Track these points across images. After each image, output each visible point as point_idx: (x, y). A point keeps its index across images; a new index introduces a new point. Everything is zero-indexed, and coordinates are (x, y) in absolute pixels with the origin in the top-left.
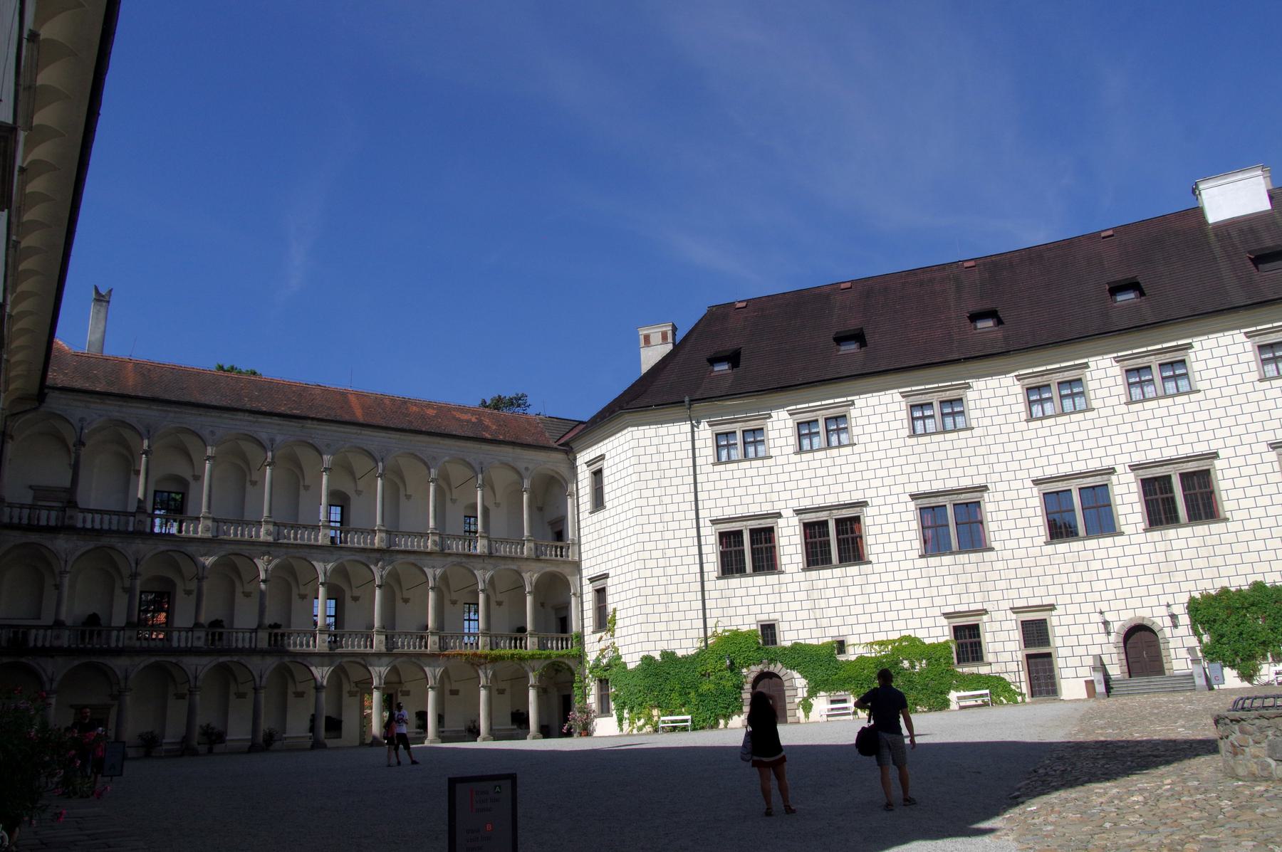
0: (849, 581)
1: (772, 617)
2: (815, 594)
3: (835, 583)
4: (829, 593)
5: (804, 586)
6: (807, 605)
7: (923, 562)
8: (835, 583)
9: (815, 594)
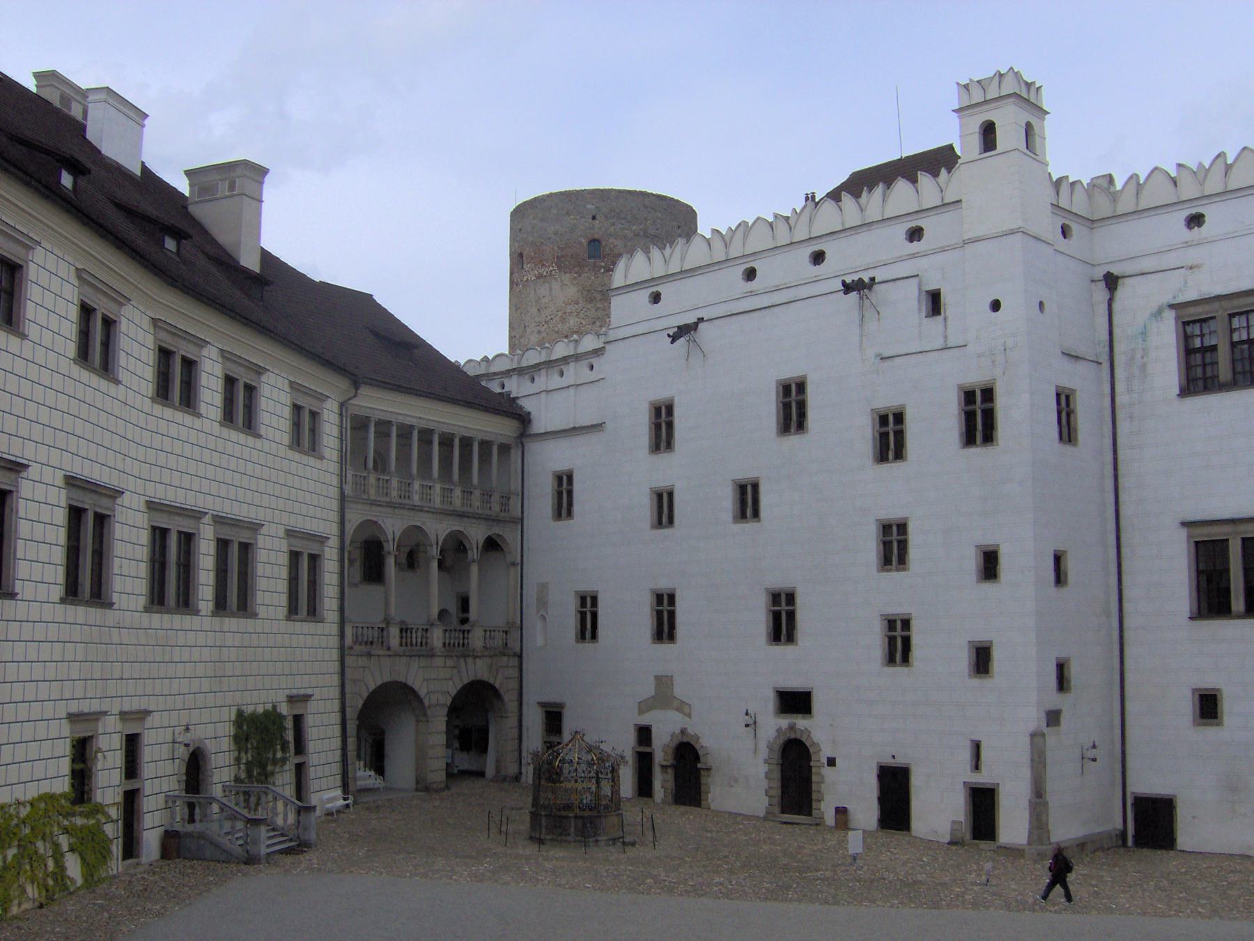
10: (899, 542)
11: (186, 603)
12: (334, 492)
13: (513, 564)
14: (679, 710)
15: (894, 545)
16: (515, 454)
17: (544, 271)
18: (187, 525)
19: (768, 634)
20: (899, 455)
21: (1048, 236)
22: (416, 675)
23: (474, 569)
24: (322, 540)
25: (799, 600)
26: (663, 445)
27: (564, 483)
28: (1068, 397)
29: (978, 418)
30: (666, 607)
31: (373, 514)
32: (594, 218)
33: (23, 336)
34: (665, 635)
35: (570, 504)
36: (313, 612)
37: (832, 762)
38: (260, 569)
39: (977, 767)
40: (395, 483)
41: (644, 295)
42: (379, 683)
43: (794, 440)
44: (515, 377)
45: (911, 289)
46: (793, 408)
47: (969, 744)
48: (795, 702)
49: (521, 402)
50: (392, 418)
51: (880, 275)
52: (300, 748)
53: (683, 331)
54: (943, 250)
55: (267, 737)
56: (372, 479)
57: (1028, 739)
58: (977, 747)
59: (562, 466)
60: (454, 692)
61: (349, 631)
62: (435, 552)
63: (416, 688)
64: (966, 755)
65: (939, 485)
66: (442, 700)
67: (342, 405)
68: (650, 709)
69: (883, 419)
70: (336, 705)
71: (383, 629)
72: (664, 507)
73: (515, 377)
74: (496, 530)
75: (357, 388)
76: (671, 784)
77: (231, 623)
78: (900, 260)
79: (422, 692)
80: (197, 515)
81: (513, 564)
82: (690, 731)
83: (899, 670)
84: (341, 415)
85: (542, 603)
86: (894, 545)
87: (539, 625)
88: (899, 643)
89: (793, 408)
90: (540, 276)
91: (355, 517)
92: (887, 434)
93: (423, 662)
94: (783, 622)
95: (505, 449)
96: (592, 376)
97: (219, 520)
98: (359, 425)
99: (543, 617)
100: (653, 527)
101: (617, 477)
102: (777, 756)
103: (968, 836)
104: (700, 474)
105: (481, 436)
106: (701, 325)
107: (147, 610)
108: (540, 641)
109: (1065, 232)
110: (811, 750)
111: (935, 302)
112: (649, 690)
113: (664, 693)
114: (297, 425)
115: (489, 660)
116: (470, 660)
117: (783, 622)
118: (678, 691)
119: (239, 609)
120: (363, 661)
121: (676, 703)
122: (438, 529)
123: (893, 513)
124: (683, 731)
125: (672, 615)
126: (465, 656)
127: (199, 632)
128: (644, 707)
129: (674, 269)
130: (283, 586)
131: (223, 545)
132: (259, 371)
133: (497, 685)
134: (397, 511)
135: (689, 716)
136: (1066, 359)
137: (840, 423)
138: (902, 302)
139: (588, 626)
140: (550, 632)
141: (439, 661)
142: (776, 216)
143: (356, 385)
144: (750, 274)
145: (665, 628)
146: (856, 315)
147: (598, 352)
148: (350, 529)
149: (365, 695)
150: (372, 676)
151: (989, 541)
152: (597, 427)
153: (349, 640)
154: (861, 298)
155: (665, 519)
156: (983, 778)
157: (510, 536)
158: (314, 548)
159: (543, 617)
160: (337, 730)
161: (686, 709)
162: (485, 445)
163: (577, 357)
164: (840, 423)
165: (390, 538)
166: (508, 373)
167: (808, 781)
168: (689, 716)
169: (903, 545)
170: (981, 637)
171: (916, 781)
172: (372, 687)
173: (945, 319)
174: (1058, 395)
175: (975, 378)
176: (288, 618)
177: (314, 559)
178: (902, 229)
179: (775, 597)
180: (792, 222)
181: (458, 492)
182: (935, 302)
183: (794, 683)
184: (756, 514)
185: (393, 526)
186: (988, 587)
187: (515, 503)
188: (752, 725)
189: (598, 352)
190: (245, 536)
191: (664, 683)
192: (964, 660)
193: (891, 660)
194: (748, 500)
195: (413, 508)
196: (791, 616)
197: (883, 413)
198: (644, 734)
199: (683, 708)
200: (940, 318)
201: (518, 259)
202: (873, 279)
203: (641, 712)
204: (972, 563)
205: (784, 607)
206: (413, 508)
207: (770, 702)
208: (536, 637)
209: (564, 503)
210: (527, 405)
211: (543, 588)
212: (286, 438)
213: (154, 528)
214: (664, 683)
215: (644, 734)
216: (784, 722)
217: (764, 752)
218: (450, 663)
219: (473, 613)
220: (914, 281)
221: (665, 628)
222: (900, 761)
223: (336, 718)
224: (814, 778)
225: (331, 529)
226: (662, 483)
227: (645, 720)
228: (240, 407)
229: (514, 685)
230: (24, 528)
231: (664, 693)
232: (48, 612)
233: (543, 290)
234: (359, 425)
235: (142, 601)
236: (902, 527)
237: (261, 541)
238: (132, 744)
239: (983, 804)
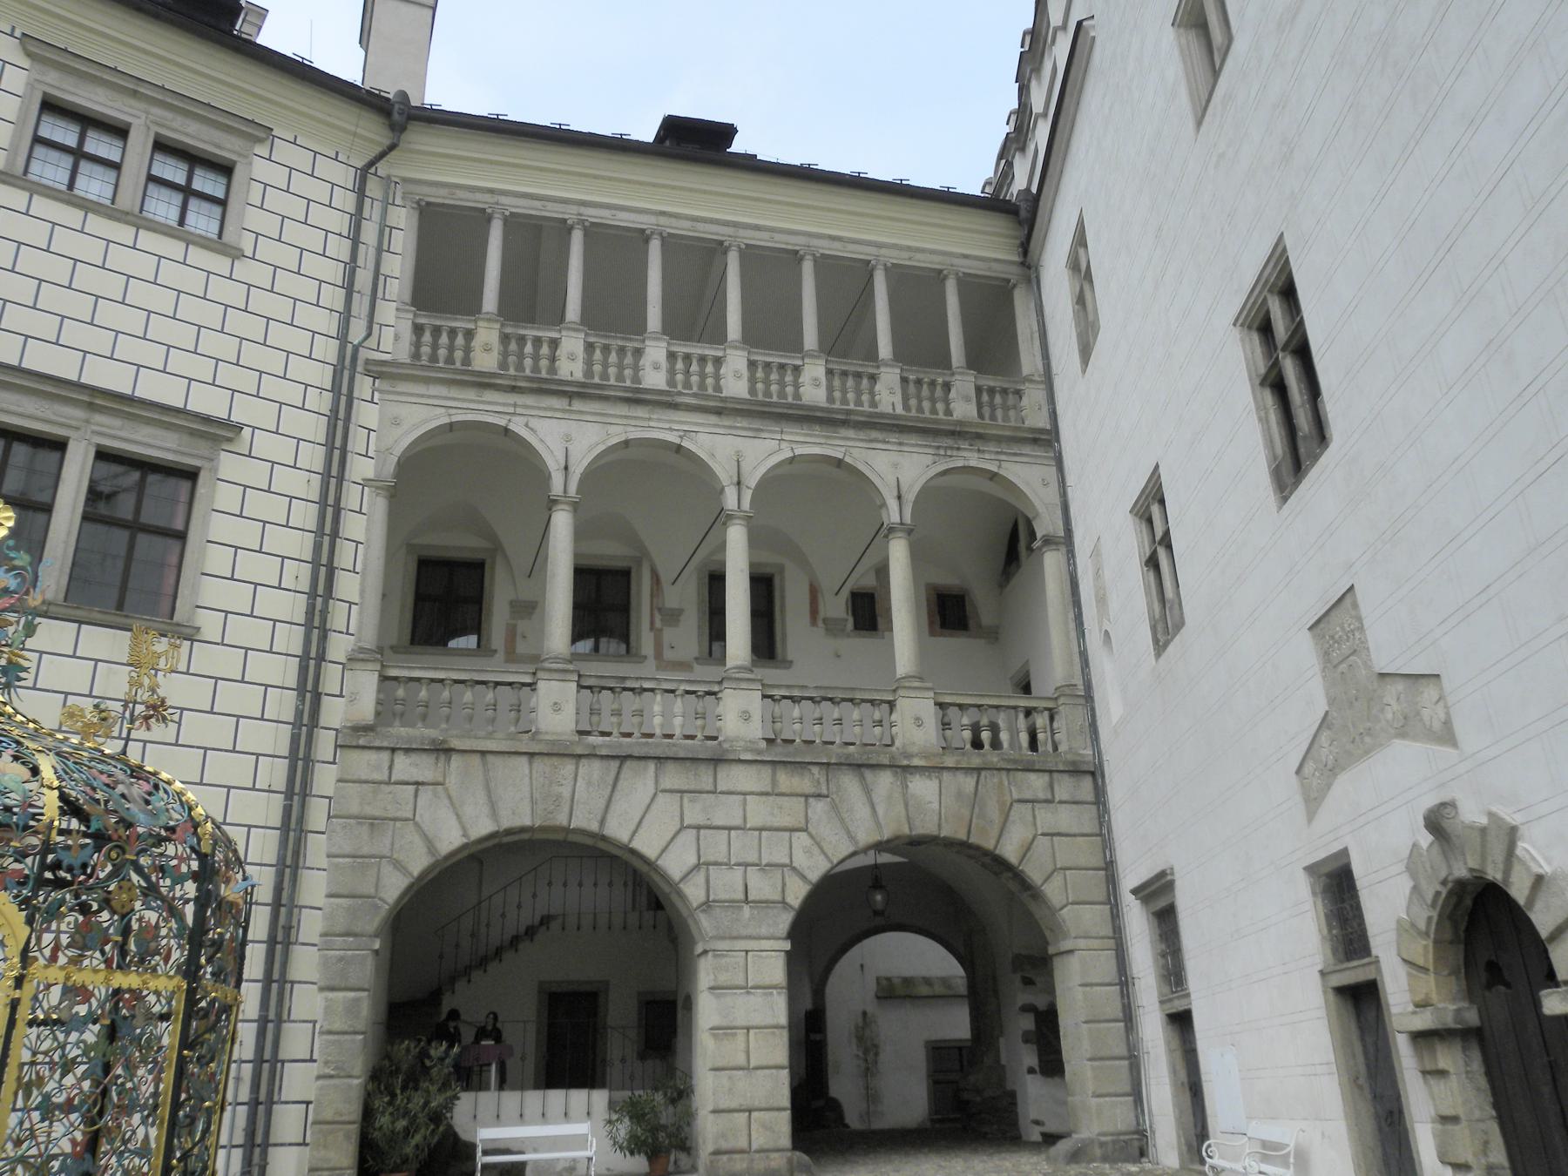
31: (489, 409)
50: (570, 213)
66: (763, 888)
81: (1049, 541)
84: (361, 193)
93: (674, 777)
115: (968, 783)
116: (884, 782)
122: (741, 457)
133: (1010, 851)
134: (578, 405)
135: (1446, 735)
157: (1026, 475)
165: (553, 464)
168: (1446, 735)
172: (450, 839)
206: (637, 398)
218: (786, 780)
229: (1084, 852)
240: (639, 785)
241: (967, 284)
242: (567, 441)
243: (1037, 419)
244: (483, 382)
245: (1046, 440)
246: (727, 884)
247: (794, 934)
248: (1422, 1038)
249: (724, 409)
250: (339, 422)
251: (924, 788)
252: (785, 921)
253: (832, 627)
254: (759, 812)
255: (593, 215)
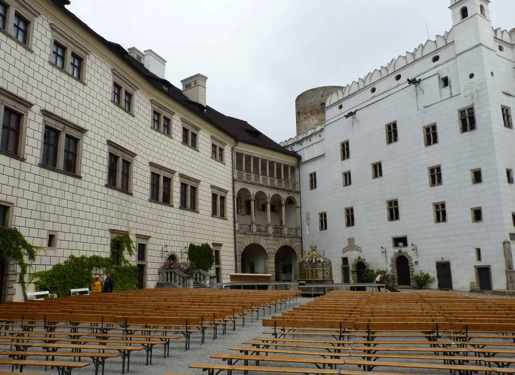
0: (66, 187)
1: (10, 199)
2: (44, 190)
3: (56, 185)
4: (52, 192)
5: (38, 179)
6: (37, 197)
7: (105, 190)
8: (56, 185)
9: (44, 190)
10: (438, 175)
11: (167, 200)
12: (231, 177)
13: (298, 207)
14: (357, 250)
15: (436, 176)
16: (297, 171)
17: (306, 116)
18: (168, 175)
19: (388, 217)
20: (435, 141)
21: (494, 48)
22: (262, 242)
23: (284, 208)
24: (226, 192)
25: (399, 203)
26: (346, 157)
27: (313, 177)
28: (507, 111)
29: (468, 121)
30: (350, 213)
31: (245, 186)
32: (322, 96)
33: (85, 84)
34: (351, 224)
35: (315, 183)
36: (223, 216)
37: (416, 263)
38: (200, 197)
39: (479, 259)
40: (253, 176)
41: (337, 107)
42: (249, 244)
43: (393, 144)
44: (296, 145)
45: (436, 79)
46: (392, 133)
47: (475, 250)
48: (400, 241)
49: (298, 153)
51: (422, 77)
52: (218, 262)
53: (351, 114)
54: (448, 61)
55: (203, 257)
56: (244, 174)
57: (502, 245)
58: (478, 251)
59: (312, 171)
60: (277, 249)
61: (237, 225)
62: (269, 200)
63: (263, 246)
64: (474, 254)
65: (454, 150)
66: (273, 251)
67: (232, 148)
68: (348, 251)
69: (428, 130)
70: (233, 250)
71: (250, 226)
72: (347, 178)
73: (296, 145)
74: (291, 195)
75: (237, 143)
76: (356, 278)
77: (189, 213)
78: (430, 69)
79: (266, 248)
80: (173, 172)
81: (298, 207)
82: (362, 257)
83: (442, 224)
85: (308, 219)
86: (436, 176)
87: (307, 227)
88: (441, 213)
89: (392, 133)
90: (305, 118)
91: (238, 187)
92: (430, 135)
94: (394, 212)
95: (293, 169)
96: (321, 139)
97: (181, 176)
98: (239, 156)
99: (308, 224)
100: (344, 186)
101: (330, 172)
102: (395, 264)
103: (478, 289)
104: (359, 164)
105: (284, 163)
106: (357, 112)
107: (150, 201)
108: (308, 233)
109: (501, 48)
110: (408, 259)
111: (446, 82)
112: (346, 244)
113: (351, 245)
114: (214, 152)
116: (283, 238)
117: (394, 212)
118: (357, 243)
119: (191, 208)
120: (243, 236)
121: (356, 248)
122: (270, 193)
123: (434, 164)
124: (359, 258)
125: (353, 216)
126: (281, 237)
127: (173, 213)
128: (345, 251)
129: (346, 95)
130: (210, 204)
131: (184, 186)
132: (198, 129)
133: (293, 248)
134: (254, 186)
135: (361, 252)
136: (504, 95)
137: (411, 134)
138: (432, 85)
139: (323, 224)
140: (311, 229)
141: (271, 238)
142: (382, 67)
143: (237, 141)
144: (373, 90)
145: (350, 221)
146: (415, 94)
147: (322, 130)
148: (237, 191)
149: (244, 248)
150: (247, 241)
151: (476, 167)
152: (323, 156)
153: (237, 228)
154: (416, 86)
155: (348, 183)
156: (483, 263)
157: (296, 198)
158: (223, 194)
159: (308, 224)
160: (233, 258)
161: (360, 249)
162: (286, 167)
163: (315, 134)
164: (411, 134)
165: (252, 195)
166: (293, 144)
167: (409, 272)
168: (361, 252)
169: (440, 176)
170: (476, 206)
171: (453, 267)
172: (247, 245)
173: (450, 87)
174: (503, 109)
175: (465, 104)
176: (212, 216)
177: (223, 199)
178: (430, 59)
179: (390, 203)
180: (388, 68)
181: (276, 181)
182: (446, 82)
183: (399, 234)
184: (381, 174)
185: (253, 191)
186: (478, 186)
187: (297, 186)
188: (385, 252)
189: (322, 130)
190: (194, 184)
191: (351, 241)
192: (469, 216)
193: (438, 220)
194: (377, 170)
195: (260, 185)
196: (397, 210)
197: (427, 127)
198: (345, 260)
199: (359, 249)
200: (448, 87)
201: (298, 114)
202: (420, 80)
203: (344, 253)
204: (469, 177)
205: (394, 206)
206: (260, 185)
207: (391, 243)
208: (306, 231)
209: (313, 184)
210: (299, 153)
211: (308, 213)
212: (210, 155)
213: (152, 173)
214: (351, 241)
215: (345, 260)
216: (397, 250)
217: (390, 262)
218: (275, 239)
219: (284, 223)
220: (437, 76)
221: (350, 221)
222: (446, 259)
223: (233, 254)
224: (410, 270)
225: (230, 189)
226: (346, 170)
227: (345, 255)
228: (190, 139)
229: (300, 248)
230: (85, 154)
231: (351, 245)
232: (98, 188)
233: (306, 122)
234: (239, 156)
235: (148, 198)
236: (439, 169)
237: (200, 187)
238: (142, 249)
239: (484, 274)
240: (262, 238)
241: (291, 167)
242: (253, 191)
243: (298, 190)
244: (245, 182)
245: (299, 192)
246: (270, 251)
247: (275, 257)
248: (352, 272)
249: (268, 187)
250: (233, 188)
251: (286, 239)
252: (274, 255)
253: (260, 210)
254: (273, 242)
255: (254, 155)
